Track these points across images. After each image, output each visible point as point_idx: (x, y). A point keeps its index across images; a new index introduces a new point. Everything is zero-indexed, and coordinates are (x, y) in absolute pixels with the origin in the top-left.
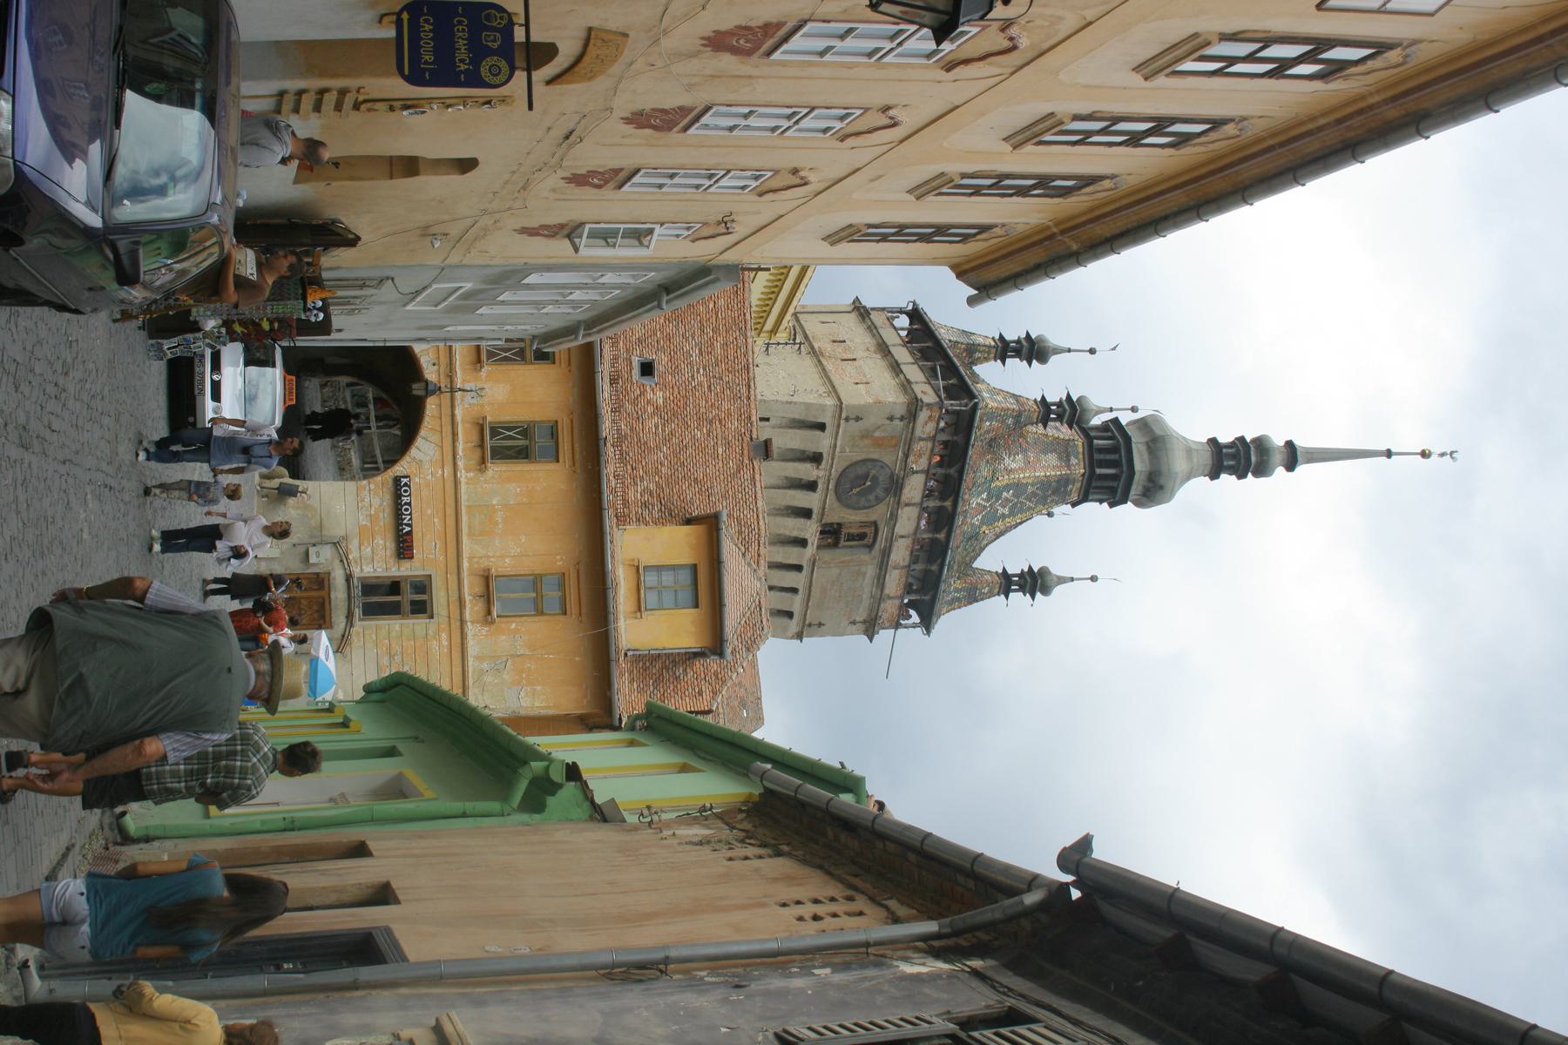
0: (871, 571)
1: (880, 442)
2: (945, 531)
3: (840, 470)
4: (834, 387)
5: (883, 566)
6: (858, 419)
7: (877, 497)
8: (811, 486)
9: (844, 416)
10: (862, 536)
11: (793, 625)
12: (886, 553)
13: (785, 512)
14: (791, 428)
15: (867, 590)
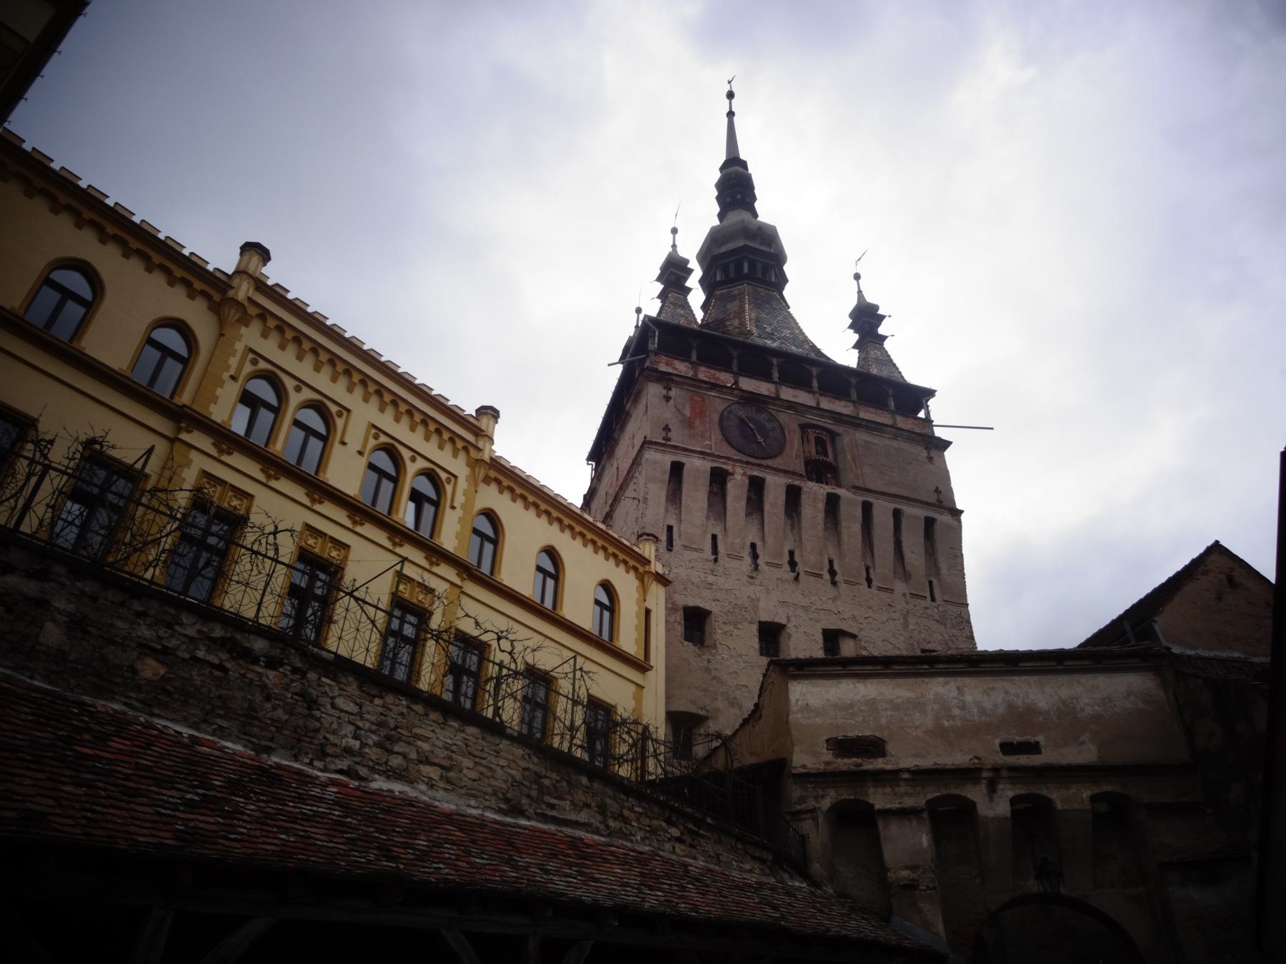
0: (862, 436)
1: (698, 411)
2: (808, 367)
3: (734, 451)
4: (633, 464)
5: (855, 423)
6: (667, 429)
7: (768, 421)
8: (756, 486)
9: (664, 442)
10: (820, 442)
11: (943, 518)
12: (838, 418)
13: (796, 519)
14: (680, 500)
15: (888, 442)
